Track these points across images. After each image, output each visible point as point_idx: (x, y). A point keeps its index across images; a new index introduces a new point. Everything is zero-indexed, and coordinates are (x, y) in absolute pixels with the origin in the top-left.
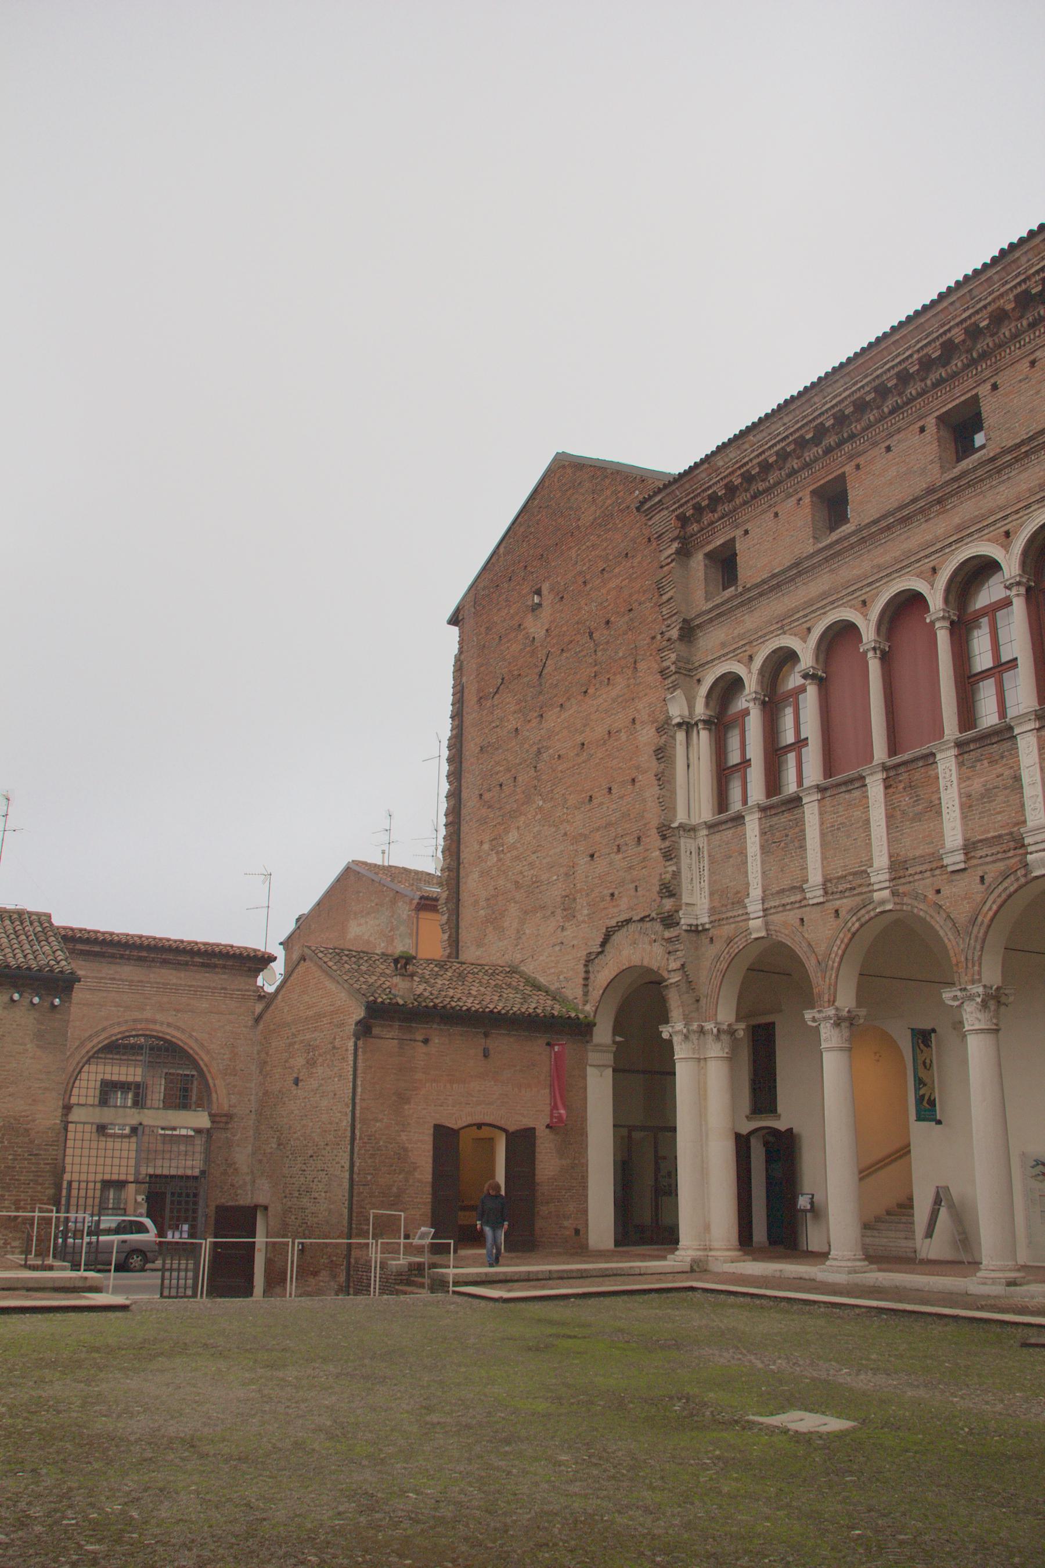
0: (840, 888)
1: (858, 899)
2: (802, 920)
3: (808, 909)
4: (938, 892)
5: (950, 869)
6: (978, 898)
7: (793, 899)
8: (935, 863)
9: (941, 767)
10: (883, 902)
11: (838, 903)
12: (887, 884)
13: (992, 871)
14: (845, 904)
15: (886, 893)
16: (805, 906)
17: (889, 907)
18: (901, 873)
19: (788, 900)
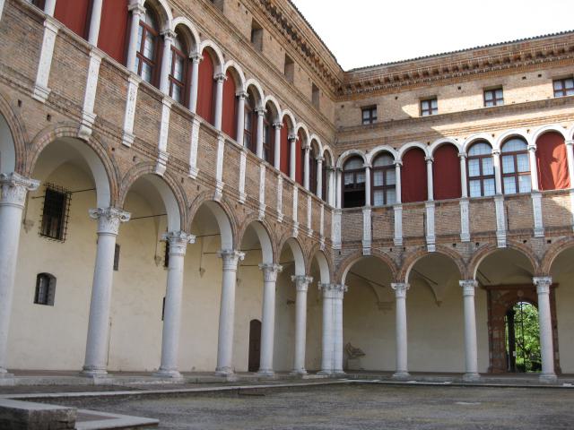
0: (59, 104)
1: (67, 119)
2: (20, 102)
3: (28, 98)
4: (113, 149)
5: (124, 142)
6: (131, 166)
7: (20, 83)
8: (120, 133)
9: (131, 86)
10: (85, 134)
11: (53, 111)
12: (91, 126)
13: (141, 158)
14: (58, 116)
15: (90, 131)
16: (26, 95)
17: (87, 139)
18: (100, 125)
19: (15, 80)
